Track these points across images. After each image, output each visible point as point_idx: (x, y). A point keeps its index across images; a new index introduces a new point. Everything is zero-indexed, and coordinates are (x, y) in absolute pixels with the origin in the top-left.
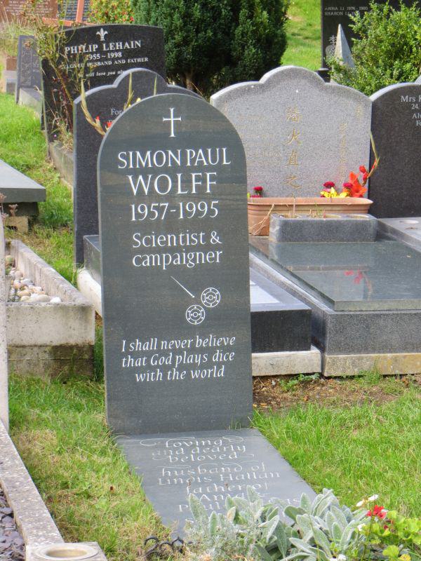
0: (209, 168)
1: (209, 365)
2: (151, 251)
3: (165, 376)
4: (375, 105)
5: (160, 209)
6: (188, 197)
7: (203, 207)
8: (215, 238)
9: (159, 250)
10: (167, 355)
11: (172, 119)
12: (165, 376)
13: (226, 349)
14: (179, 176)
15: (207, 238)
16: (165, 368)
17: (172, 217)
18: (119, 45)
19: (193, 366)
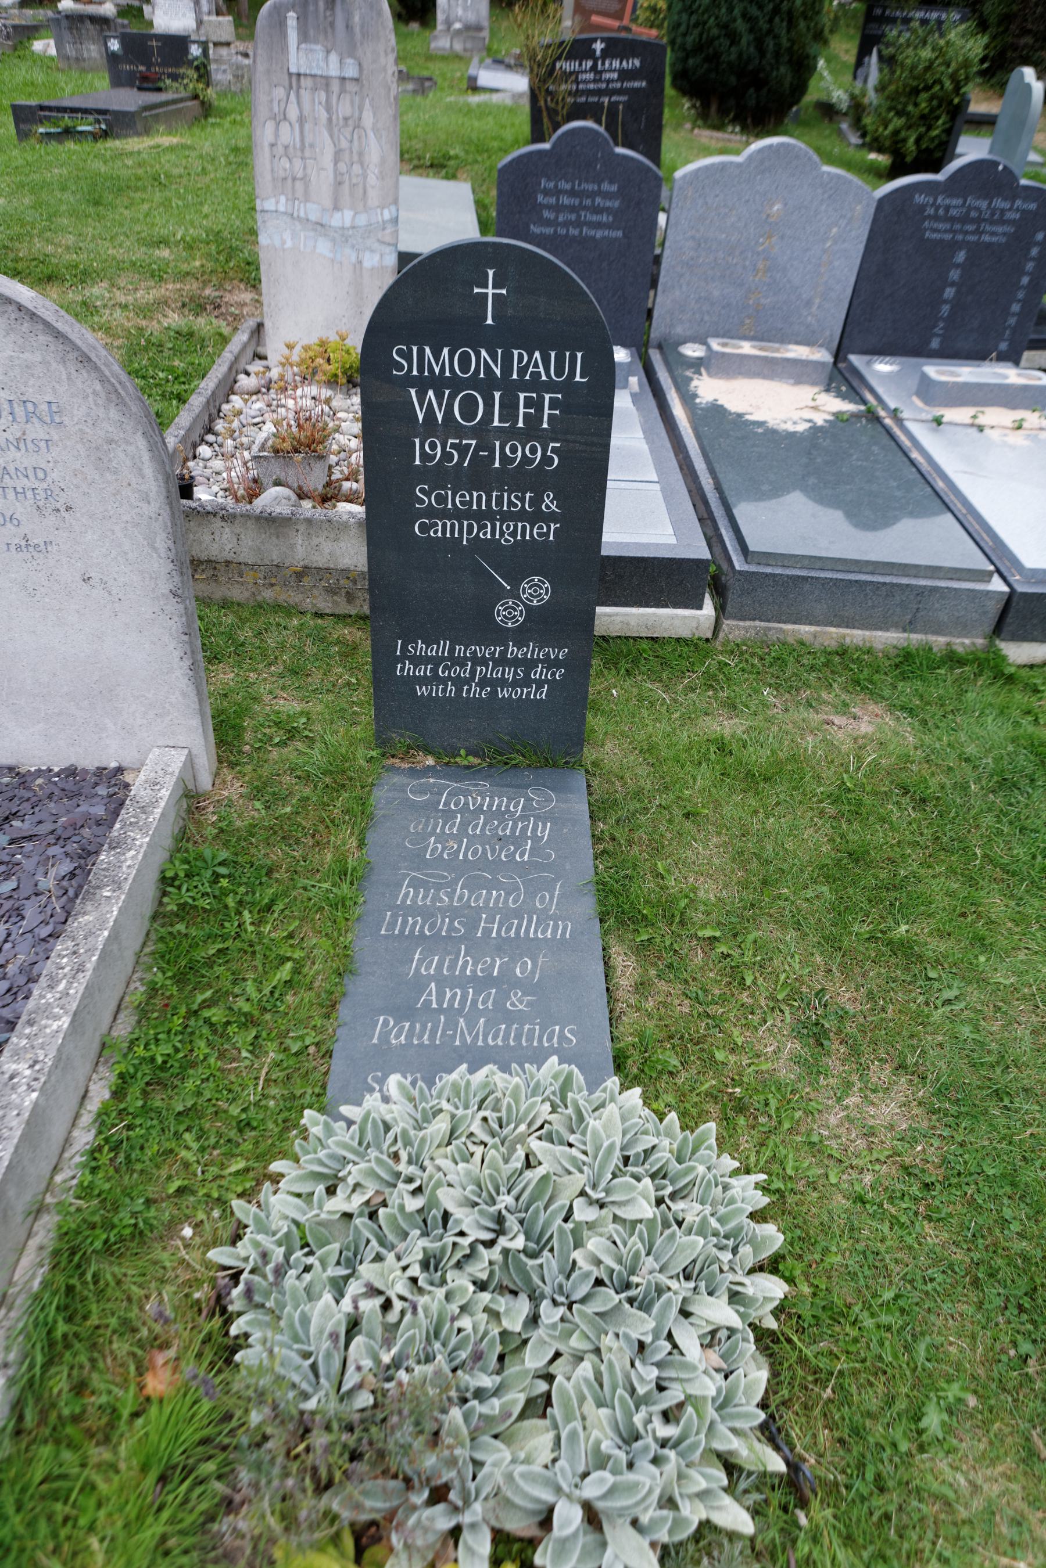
0: (550, 386)
1: (527, 682)
2: (444, 514)
3: (459, 691)
4: (881, 201)
5: (463, 450)
6: (509, 434)
7: (533, 450)
8: (549, 503)
9: (458, 515)
10: (463, 665)
11: (490, 291)
12: (459, 691)
13: (551, 664)
14: (497, 395)
15: (536, 502)
16: (459, 682)
17: (481, 464)
18: (616, 64)
19: (503, 682)
